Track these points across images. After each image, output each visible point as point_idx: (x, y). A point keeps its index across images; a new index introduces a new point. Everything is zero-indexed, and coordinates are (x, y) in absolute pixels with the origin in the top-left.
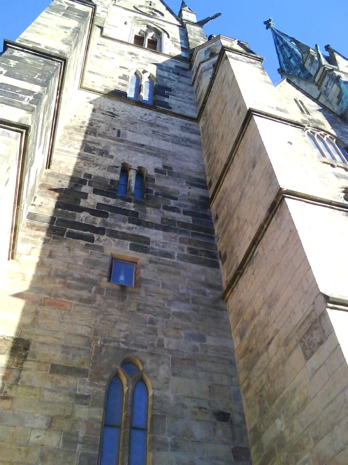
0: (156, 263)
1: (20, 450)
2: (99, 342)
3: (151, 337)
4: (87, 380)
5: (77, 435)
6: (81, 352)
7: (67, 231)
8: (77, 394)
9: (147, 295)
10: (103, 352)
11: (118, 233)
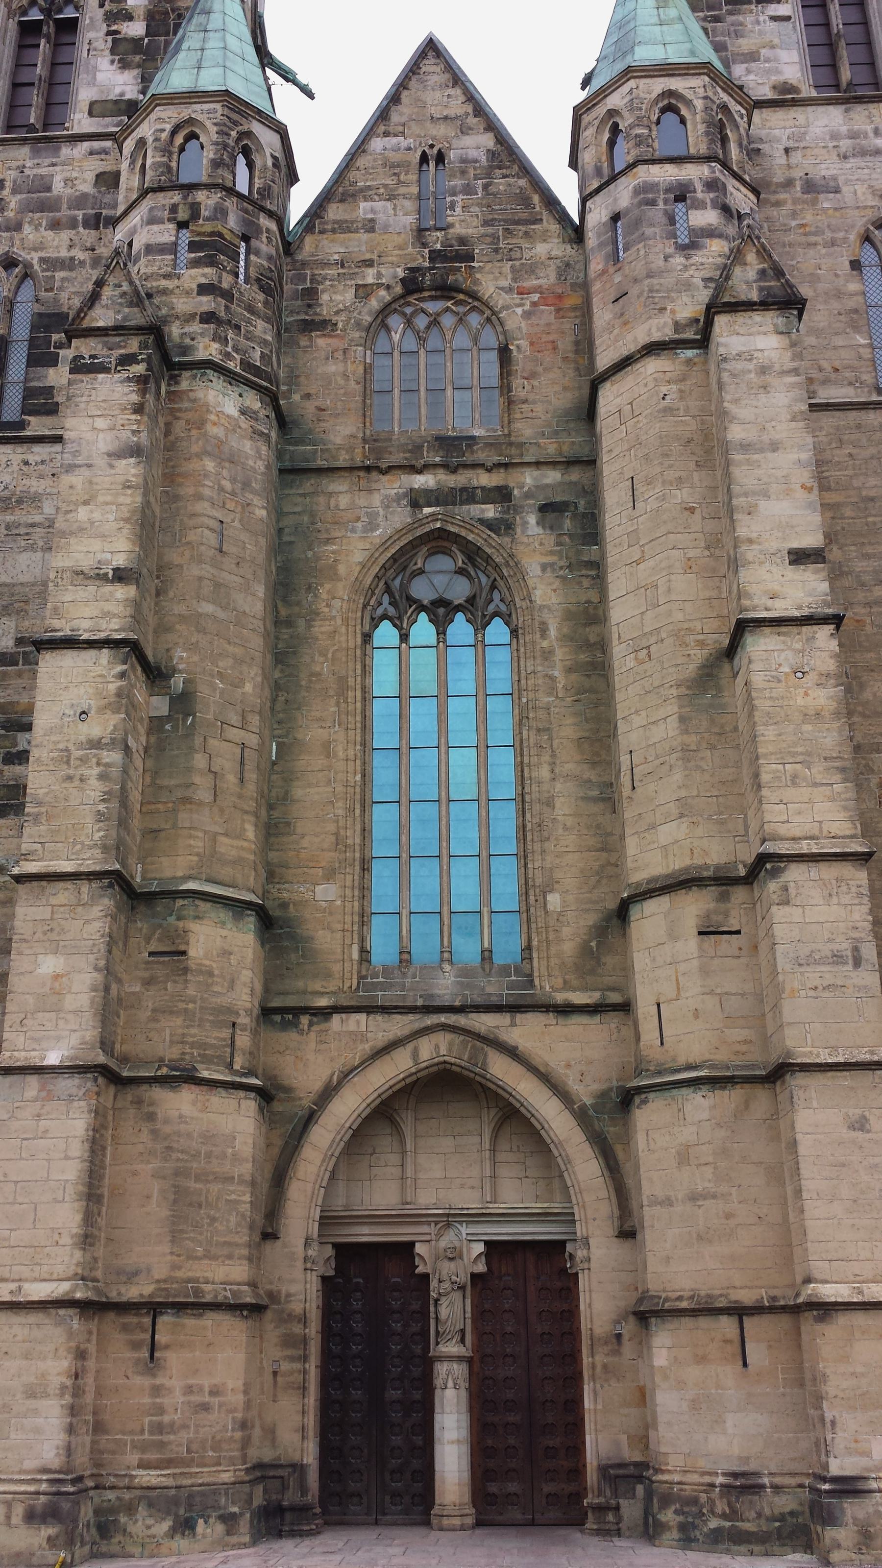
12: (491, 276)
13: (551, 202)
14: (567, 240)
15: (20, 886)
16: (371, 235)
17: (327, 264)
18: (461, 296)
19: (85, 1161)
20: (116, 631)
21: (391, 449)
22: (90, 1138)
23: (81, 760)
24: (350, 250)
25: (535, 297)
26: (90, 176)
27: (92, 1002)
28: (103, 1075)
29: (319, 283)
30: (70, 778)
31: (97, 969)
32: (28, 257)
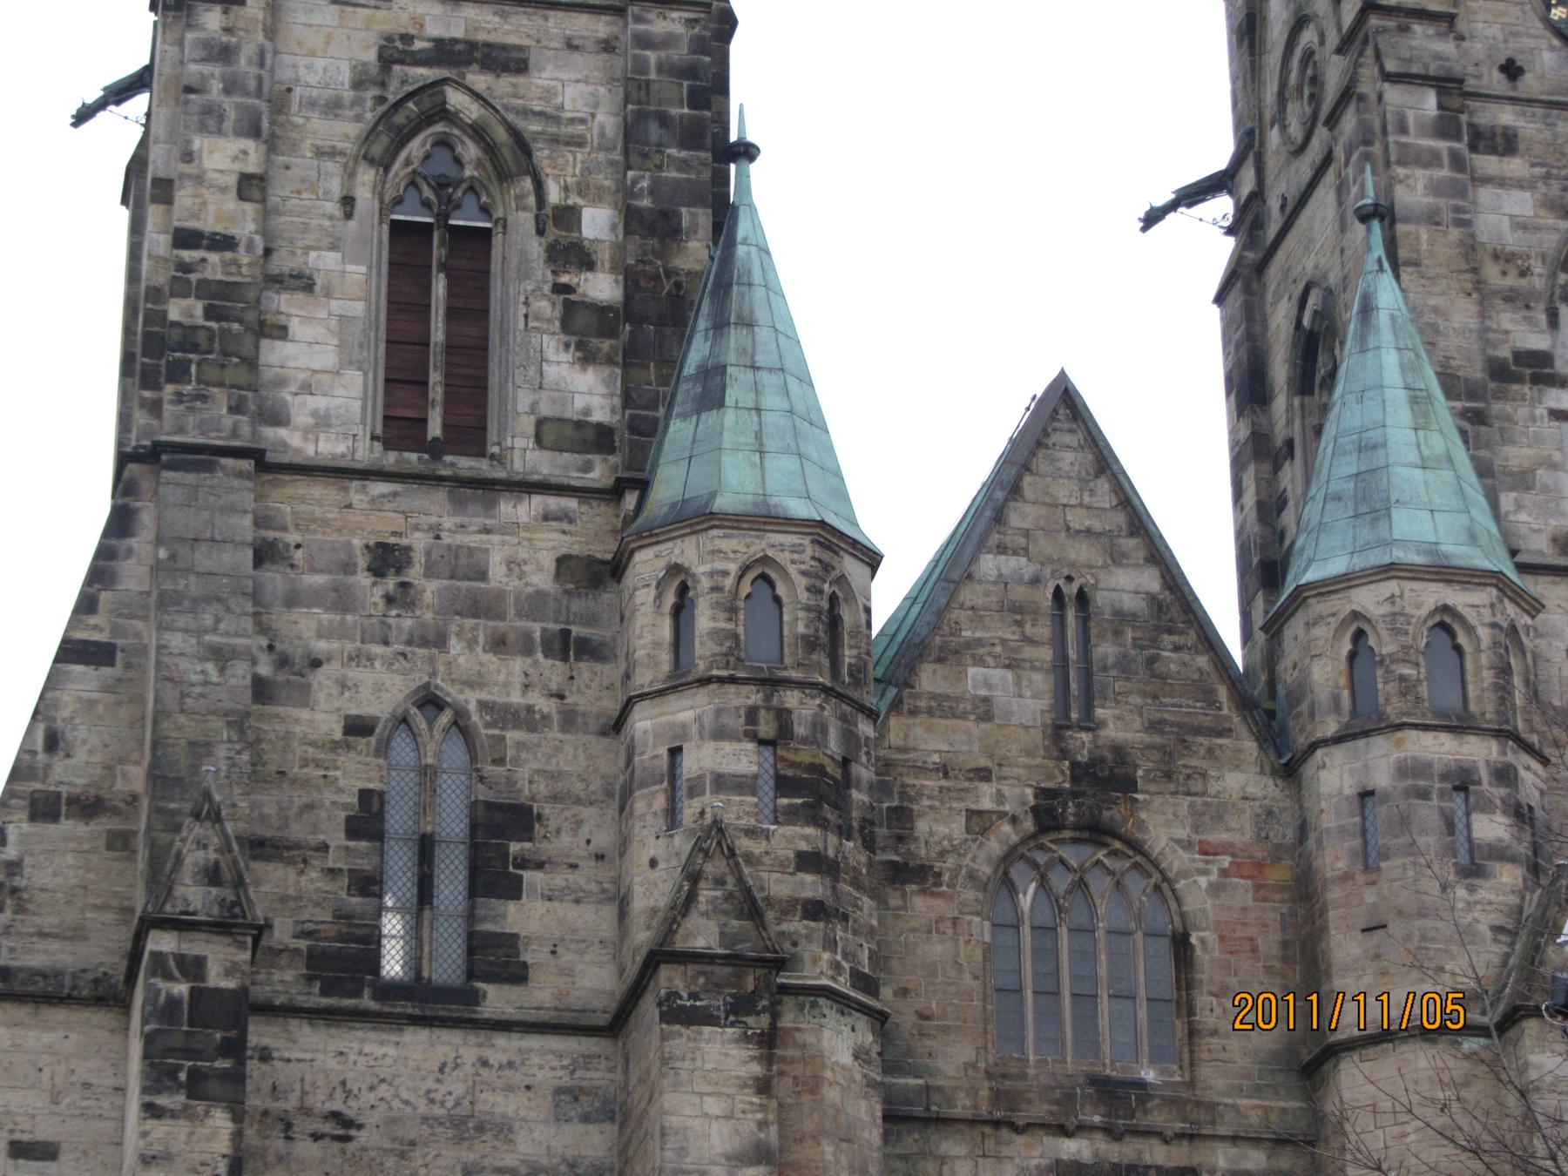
12: (1162, 818)
13: (1209, 641)
14: (1267, 769)
16: (983, 726)
17: (923, 770)
18: (1118, 845)
21: (1031, 1096)
24: (957, 747)
25: (1226, 861)
26: (548, 561)
29: (911, 800)
32: (461, 697)
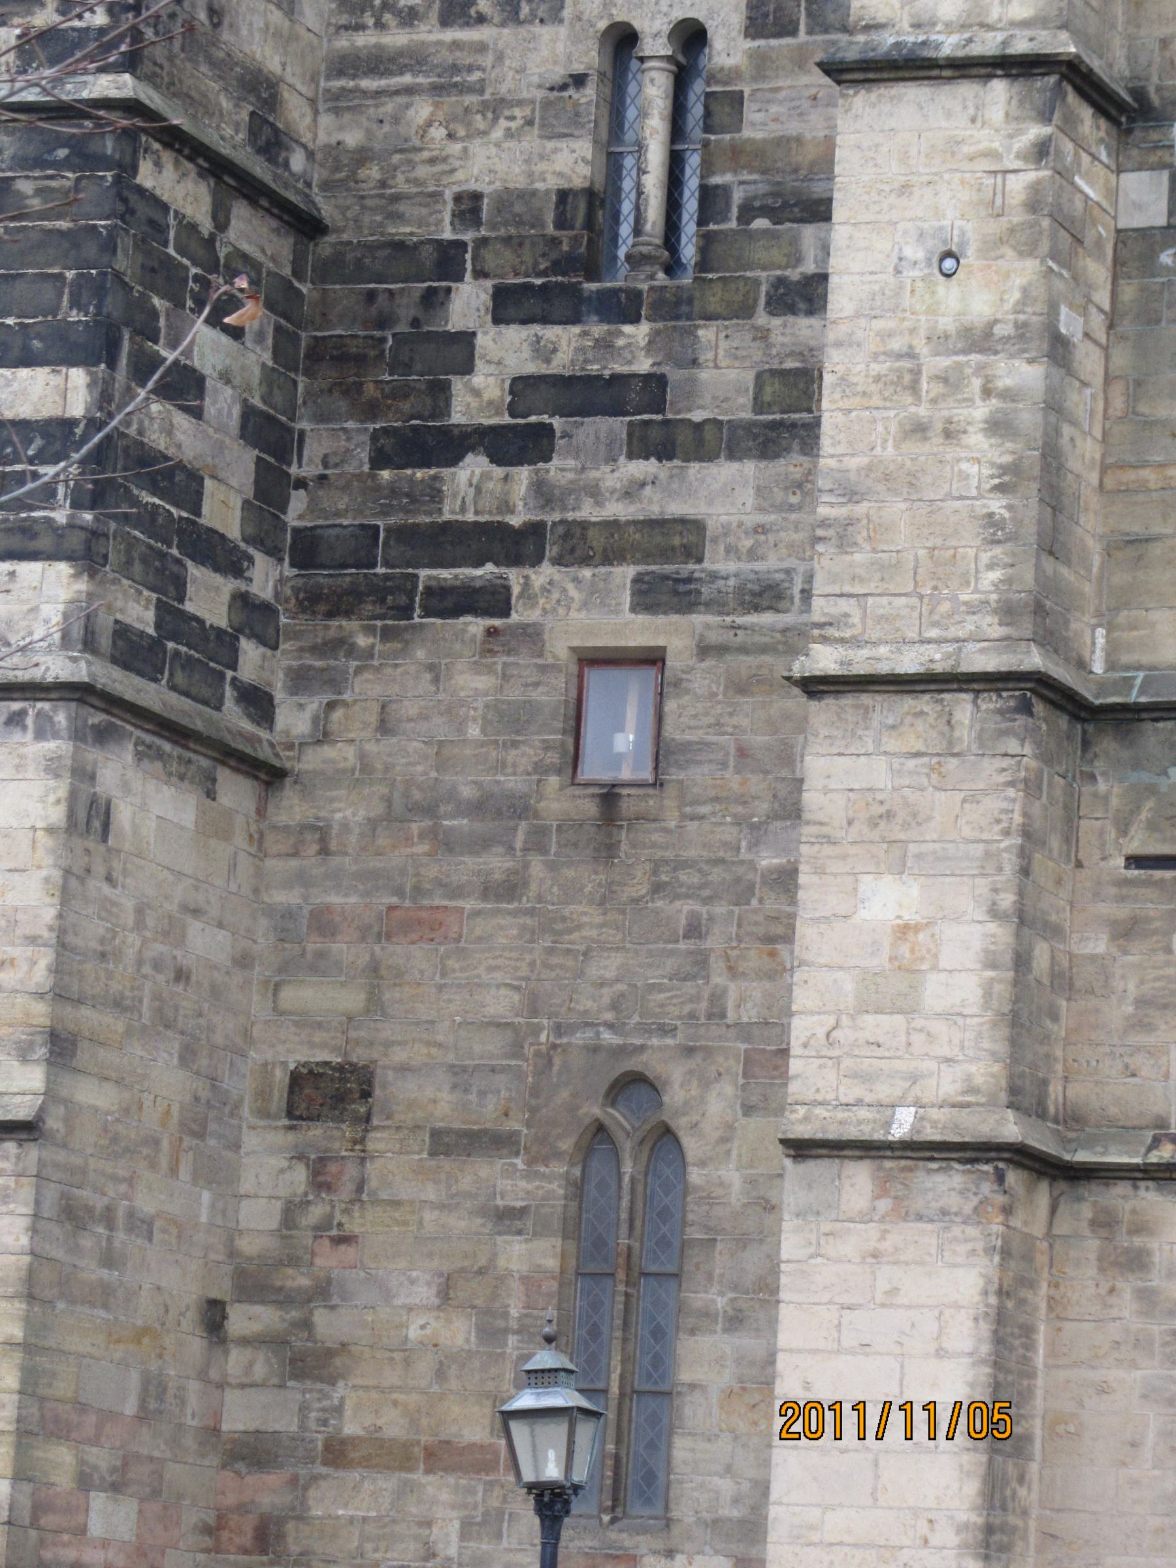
0: (721, 650)
1: (392, 1359)
2: (543, 1038)
3: (689, 988)
4: (519, 1162)
5: (505, 1315)
6: (501, 1080)
7: (421, 588)
8: (497, 1207)
9: (684, 817)
10: (556, 1068)
11: (591, 533)
15: (814, 705)
19: (983, 1362)
20: (1025, 24)
22: (992, 1312)
23: (946, 381)
27: (988, 994)
28: (1018, 1165)
30: (919, 429)
31: (994, 913)
